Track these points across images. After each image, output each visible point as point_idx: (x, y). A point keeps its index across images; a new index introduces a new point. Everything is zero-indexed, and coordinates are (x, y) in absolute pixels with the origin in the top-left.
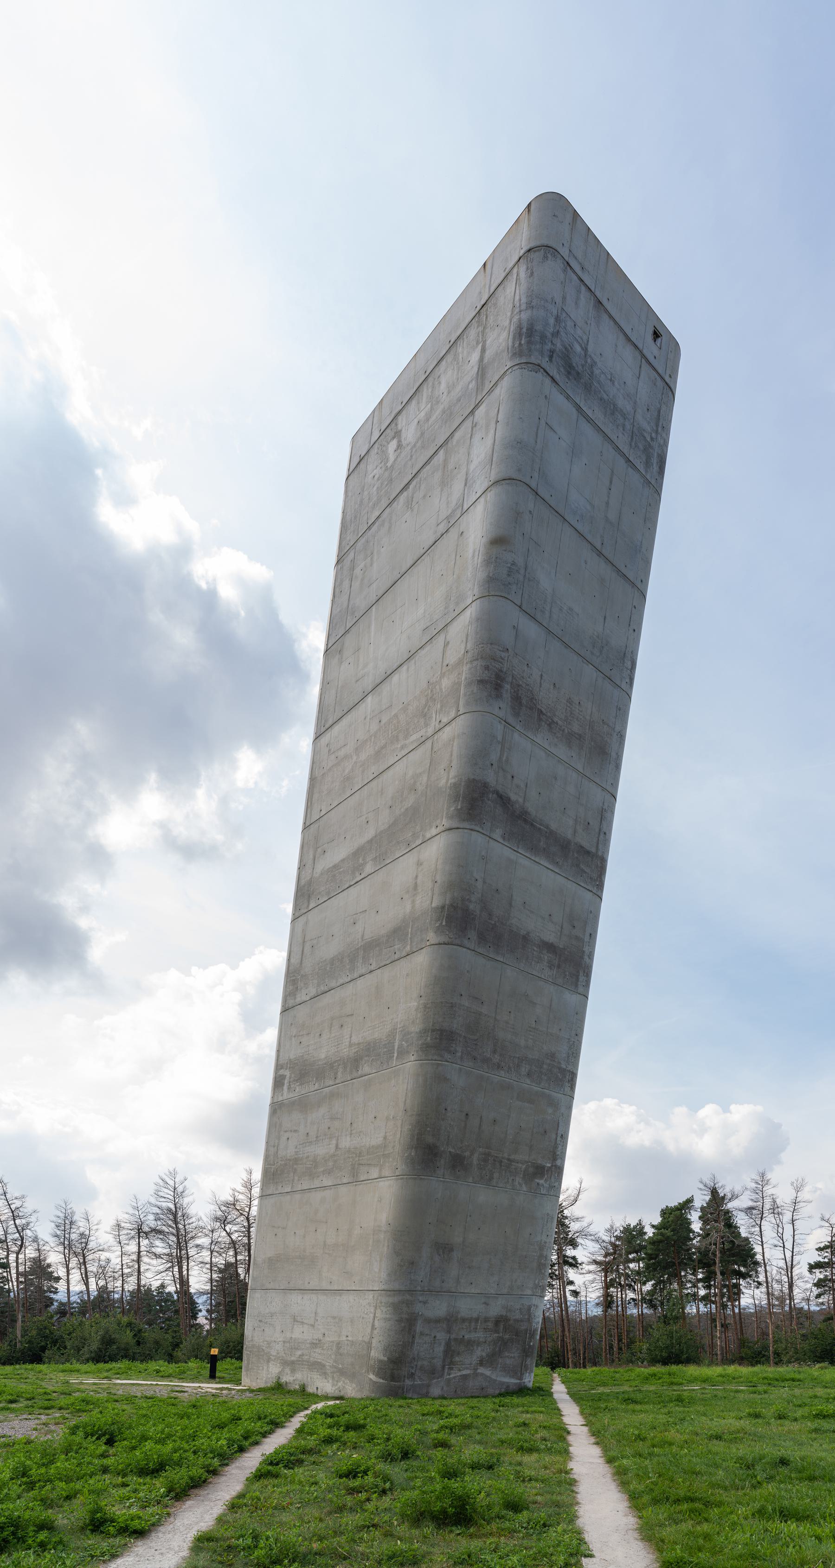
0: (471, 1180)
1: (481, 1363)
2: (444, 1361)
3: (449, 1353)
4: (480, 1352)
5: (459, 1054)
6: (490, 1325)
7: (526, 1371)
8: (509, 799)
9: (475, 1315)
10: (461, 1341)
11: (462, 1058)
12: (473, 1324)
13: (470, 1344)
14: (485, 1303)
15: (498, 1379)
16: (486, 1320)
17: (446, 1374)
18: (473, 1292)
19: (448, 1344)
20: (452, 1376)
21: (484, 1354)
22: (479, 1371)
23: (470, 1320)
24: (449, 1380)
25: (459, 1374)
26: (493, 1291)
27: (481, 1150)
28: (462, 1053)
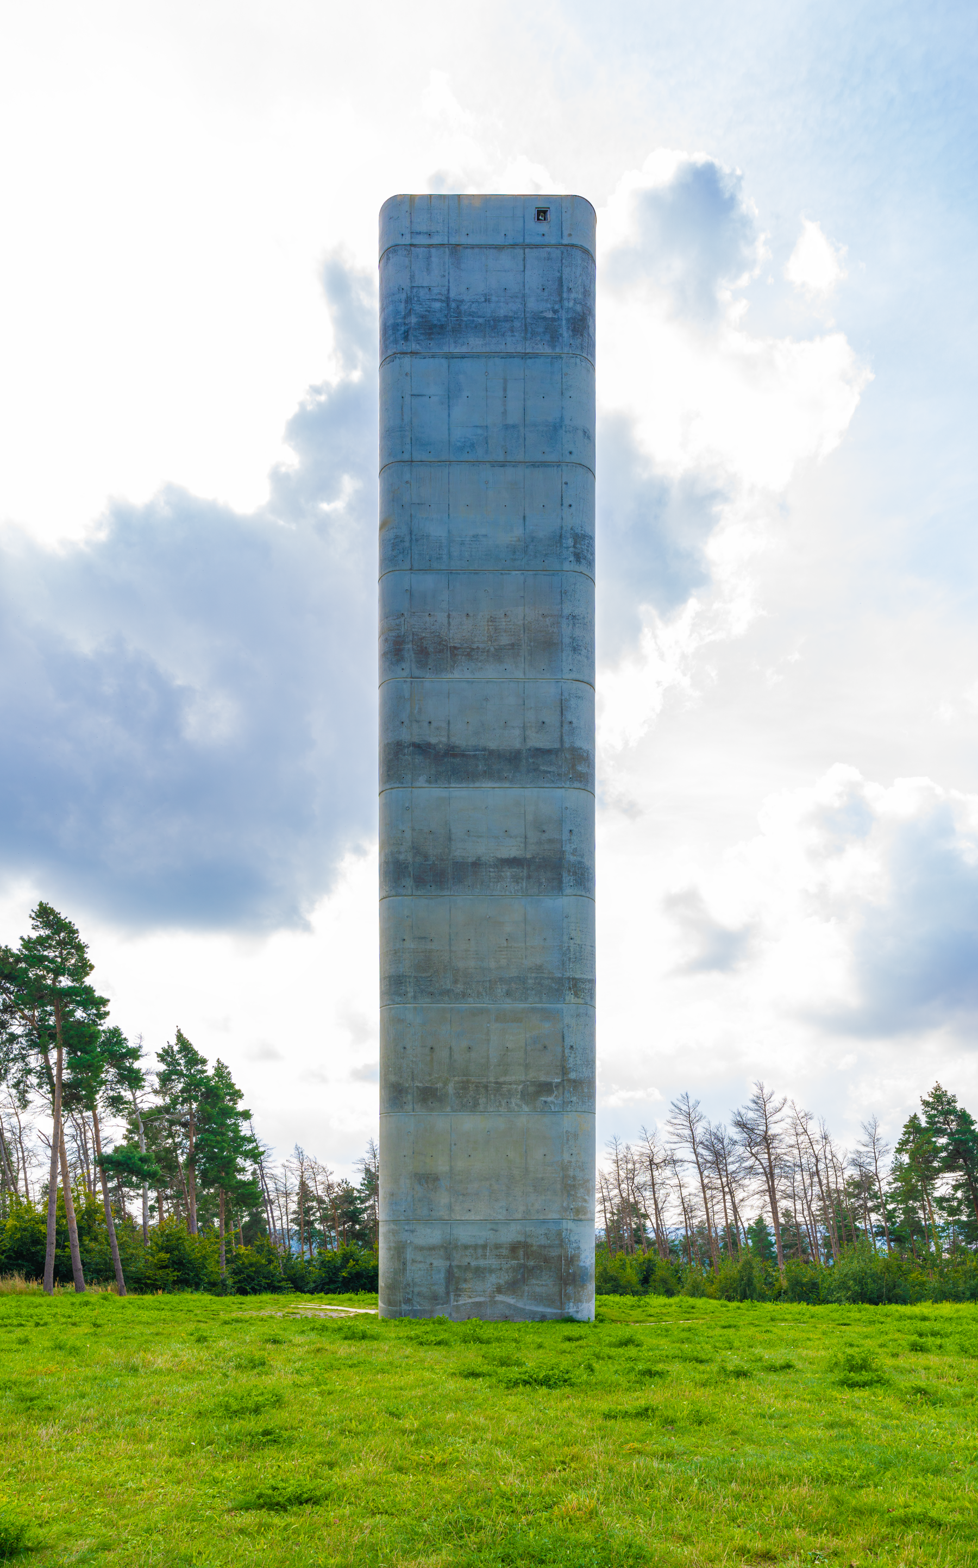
0: (449, 1109)
1: (499, 1290)
2: (447, 1287)
3: (453, 1280)
4: (493, 1280)
5: (410, 995)
6: (505, 1252)
7: (569, 1300)
8: (429, 745)
9: (481, 1242)
10: (468, 1267)
11: (415, 997)
12: (480, 1251)
13: (479, 1272)
14: (492, 1229)
15: (527, 1307)
16: (498, 1246)
17: (452, 1300)
18: (473, 1218)
19: (450, 1272)
20: (460, 1303)
21: (502, 1282)
22: (497, 1298)
23: (475, 1247)
24: (457, 1308)
25: (470, 1301)
26: (500, 1217)
27: (456, 1079)
28: (415, 992)
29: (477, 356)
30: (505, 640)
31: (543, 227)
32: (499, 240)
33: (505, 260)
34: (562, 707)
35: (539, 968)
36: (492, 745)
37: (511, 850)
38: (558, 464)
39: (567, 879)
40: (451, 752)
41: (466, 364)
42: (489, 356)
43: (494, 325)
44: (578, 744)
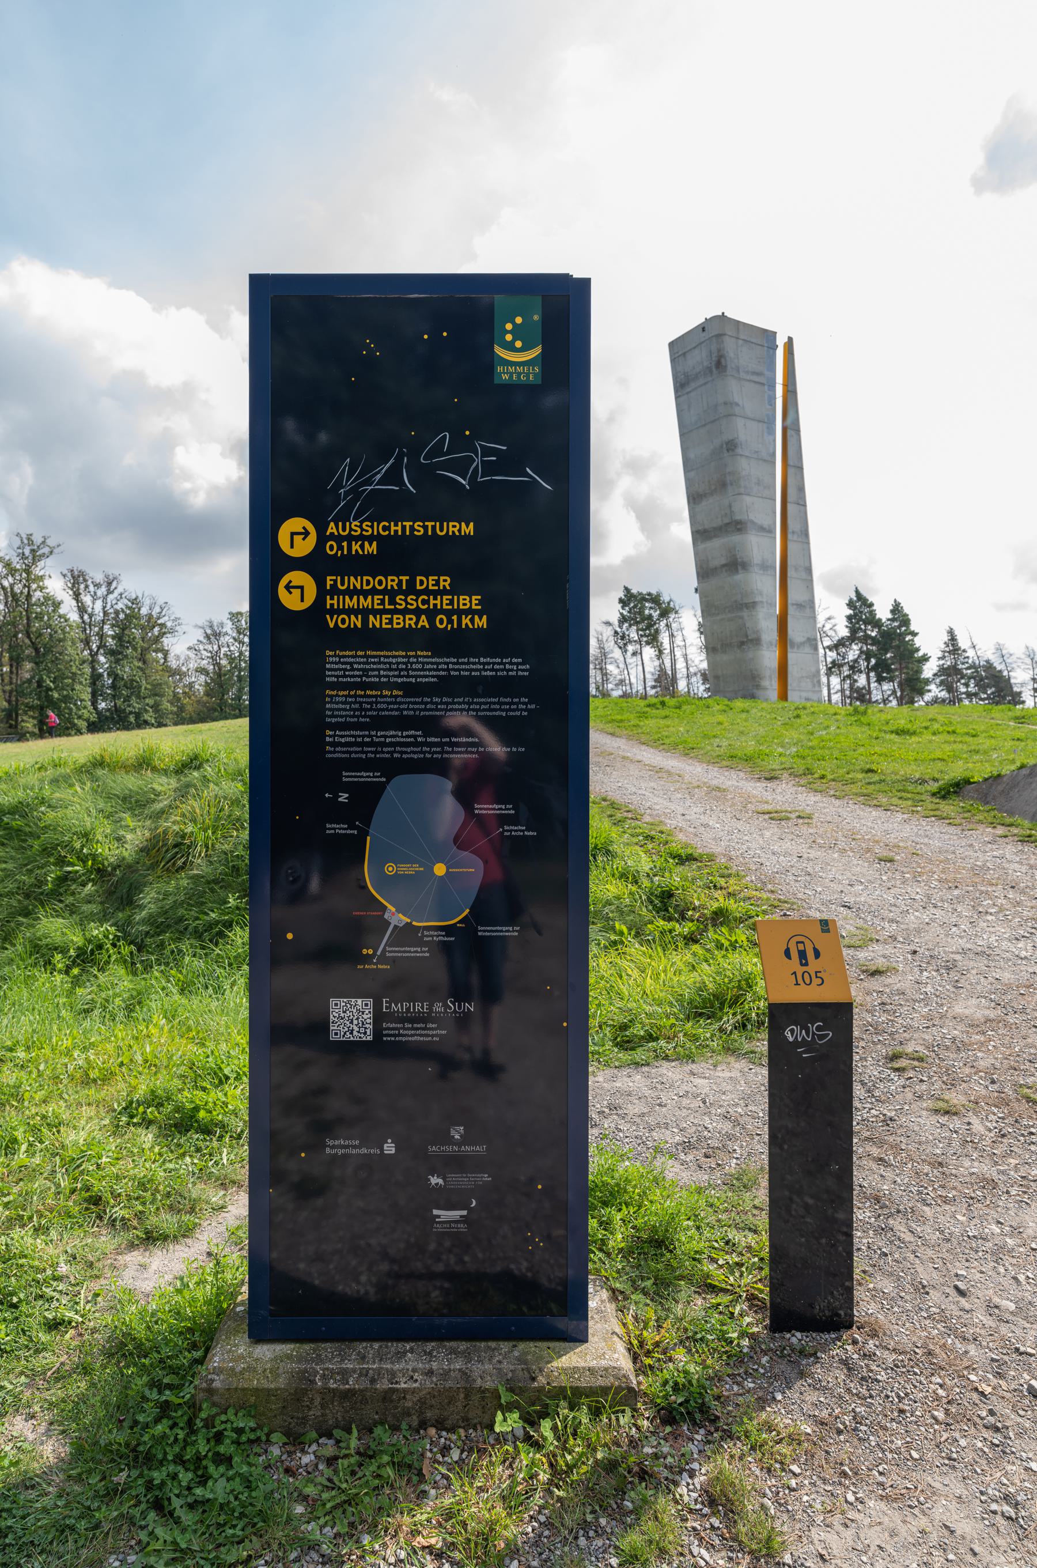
29: (693, 390)
30: (713, 487)
31: (704, 334)
32: (694, 345)
33: (696, 351)
34: (730, 506)
35: (736, 601)
36: (715, 525)
37: (723, 561)
38: (718, 419)
39: (739, 568)
40: (705, 531)
41: (693, 394)
42: (696, 388)
43: (696, 377)
44: (738, 517)
